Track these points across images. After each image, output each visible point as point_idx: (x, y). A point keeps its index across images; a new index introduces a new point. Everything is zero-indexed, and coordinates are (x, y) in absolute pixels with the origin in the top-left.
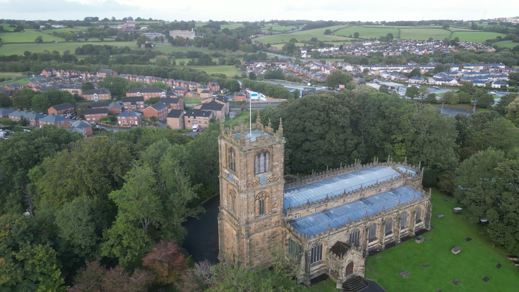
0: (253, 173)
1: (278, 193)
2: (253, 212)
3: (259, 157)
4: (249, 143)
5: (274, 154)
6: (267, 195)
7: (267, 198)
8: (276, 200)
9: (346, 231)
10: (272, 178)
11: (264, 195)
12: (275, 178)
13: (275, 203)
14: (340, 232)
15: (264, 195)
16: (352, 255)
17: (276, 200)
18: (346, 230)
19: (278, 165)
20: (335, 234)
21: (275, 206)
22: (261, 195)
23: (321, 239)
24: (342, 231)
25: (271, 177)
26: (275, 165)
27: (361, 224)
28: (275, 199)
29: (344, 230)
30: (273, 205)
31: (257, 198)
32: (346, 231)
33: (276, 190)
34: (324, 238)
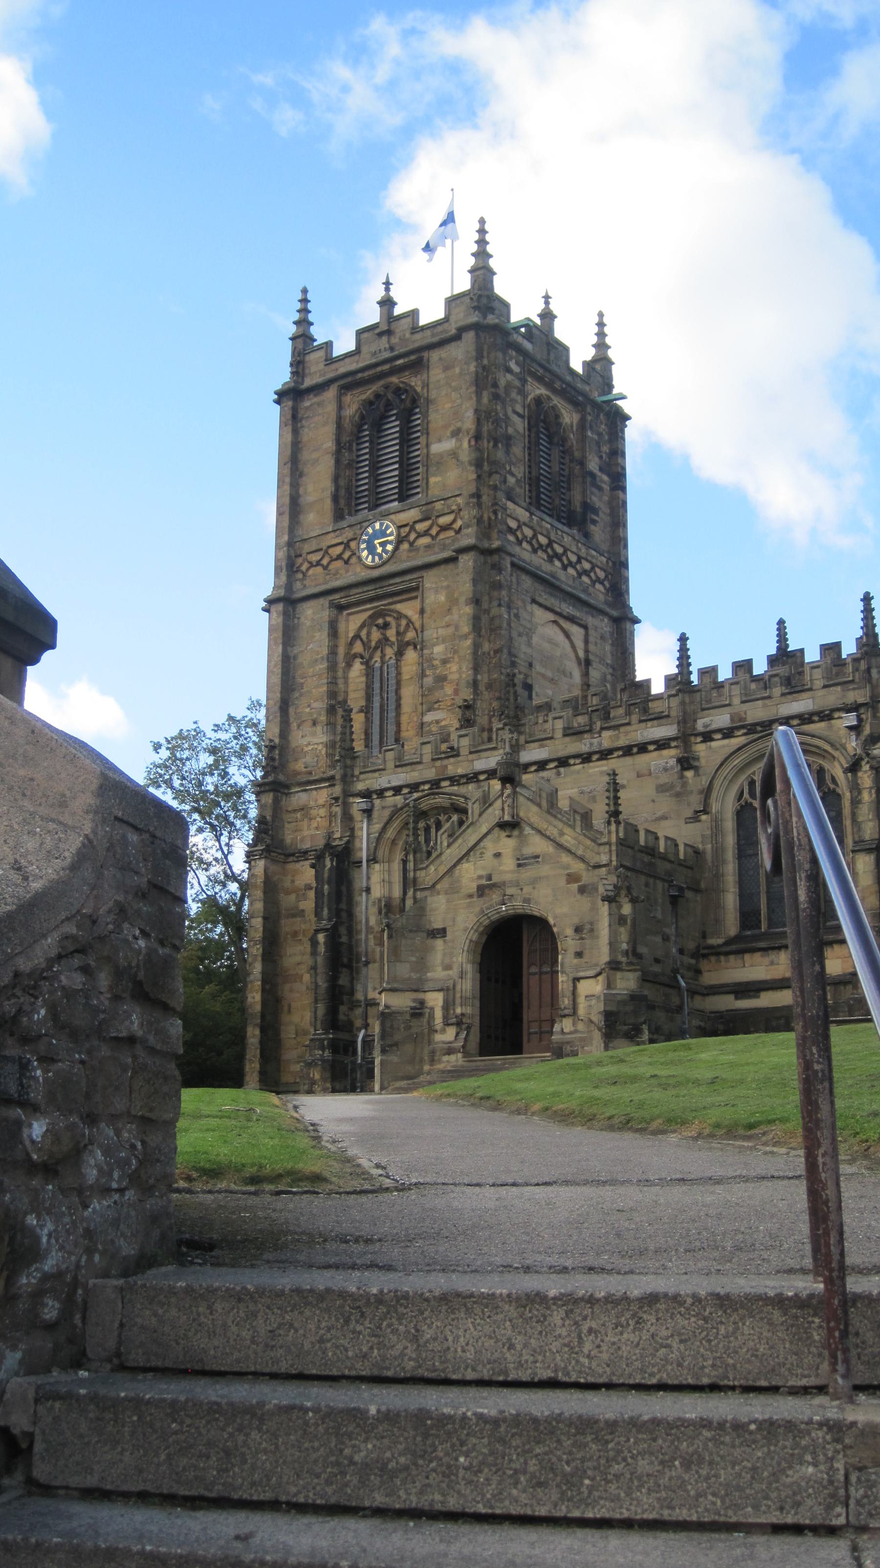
0: (328, 503)
1: (455, 610)
2: (323, 718)
3: (378, 427)
4: (321, 366)
5: (433, 394)
6: (410, 635)
7: (411, 655)
8: (445, 662)
9: (670, 756)
10: (426, 533)
11: (391, 633)
12: (444, 528)
13: (441, 679)
14: (605, 754)
15: (391, 633)
16: (507, 844)
17: (445, 662)
18: (662, 745)
19: (454, 454)
20: (563, 762)
21: (438, 694)
22: (376, 635)
23: (454, 780)
24: (627, 751)
25: (421, 527)
26: (441, 455)
27: (826, 716)
28: (438, 650)
29: (643, 748)
30: (431, 690)
31: (358, 648)
32: (670, 756)
33: (442, 598)
34: (473, 778)
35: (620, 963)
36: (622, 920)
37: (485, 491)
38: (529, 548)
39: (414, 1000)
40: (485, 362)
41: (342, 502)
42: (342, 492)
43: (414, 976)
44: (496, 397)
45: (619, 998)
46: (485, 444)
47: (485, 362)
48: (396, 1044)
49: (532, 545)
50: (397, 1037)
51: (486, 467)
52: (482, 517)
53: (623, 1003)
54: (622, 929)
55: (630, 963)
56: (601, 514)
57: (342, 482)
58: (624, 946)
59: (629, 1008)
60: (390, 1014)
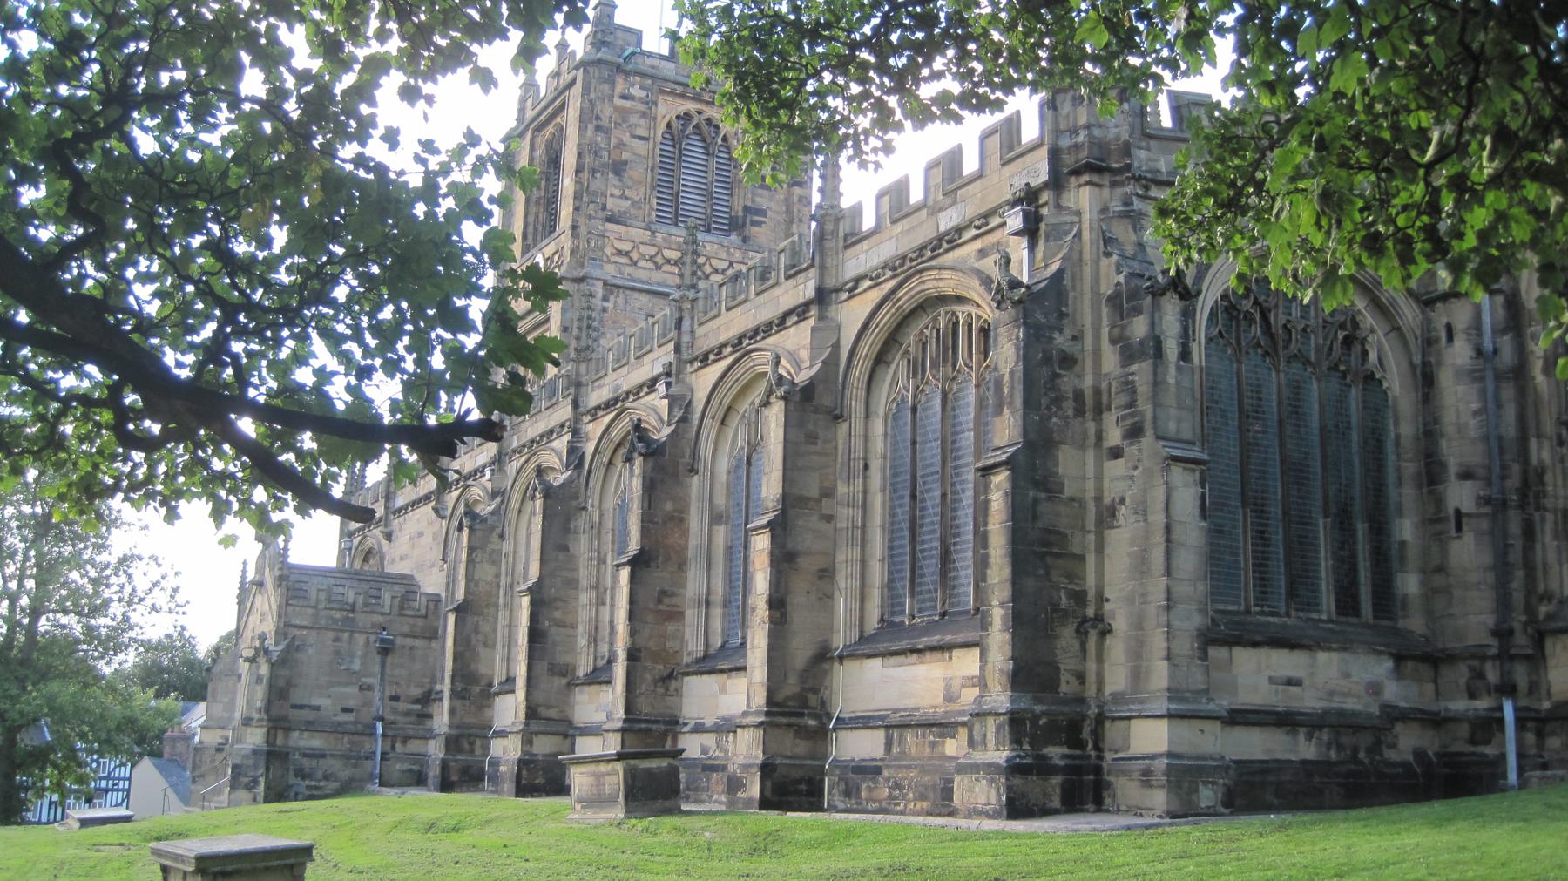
35: (251, 719)
36: (259, 679)
37: (582, 221)
38: (651, 265)
39: (221, 737)
40: (592, 96)
41: (530, 237)
42: (531, 229)
43: (226, 715)
44: (598, 128)
45: (243, 752)
46: (585, 175)
47: (592, 96)
48: (202, 776)
49: (655, 263)
50: (204, 768)
51: (585, 198)
52: (578, 247)
53: (245, 757)
54: (258, 688)
55: (260, 720)
56: (769, 213)
57: (531, 219)
58: (259, 704)
59: (251, 762)
60: (201, 749)
